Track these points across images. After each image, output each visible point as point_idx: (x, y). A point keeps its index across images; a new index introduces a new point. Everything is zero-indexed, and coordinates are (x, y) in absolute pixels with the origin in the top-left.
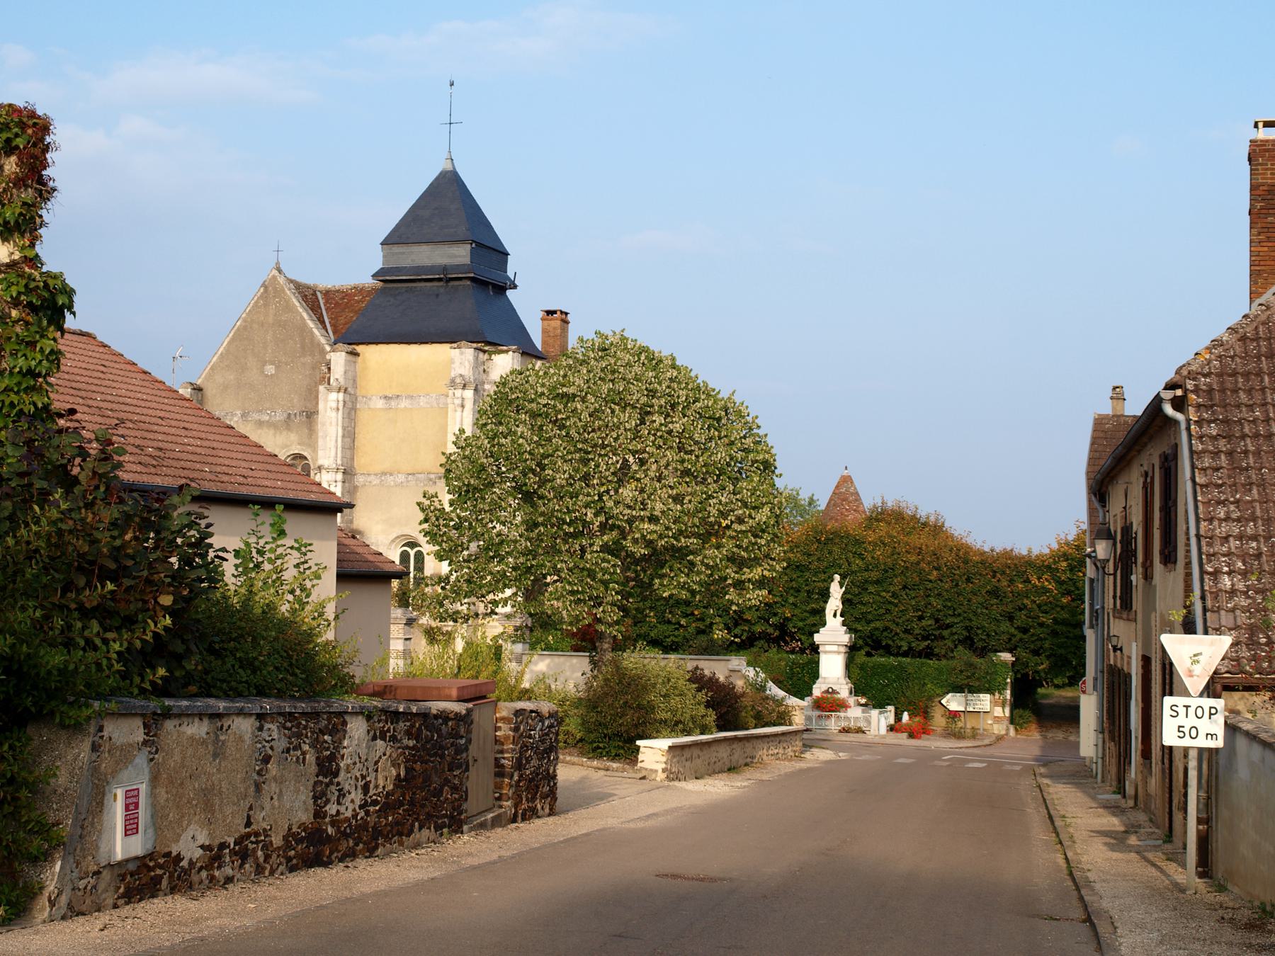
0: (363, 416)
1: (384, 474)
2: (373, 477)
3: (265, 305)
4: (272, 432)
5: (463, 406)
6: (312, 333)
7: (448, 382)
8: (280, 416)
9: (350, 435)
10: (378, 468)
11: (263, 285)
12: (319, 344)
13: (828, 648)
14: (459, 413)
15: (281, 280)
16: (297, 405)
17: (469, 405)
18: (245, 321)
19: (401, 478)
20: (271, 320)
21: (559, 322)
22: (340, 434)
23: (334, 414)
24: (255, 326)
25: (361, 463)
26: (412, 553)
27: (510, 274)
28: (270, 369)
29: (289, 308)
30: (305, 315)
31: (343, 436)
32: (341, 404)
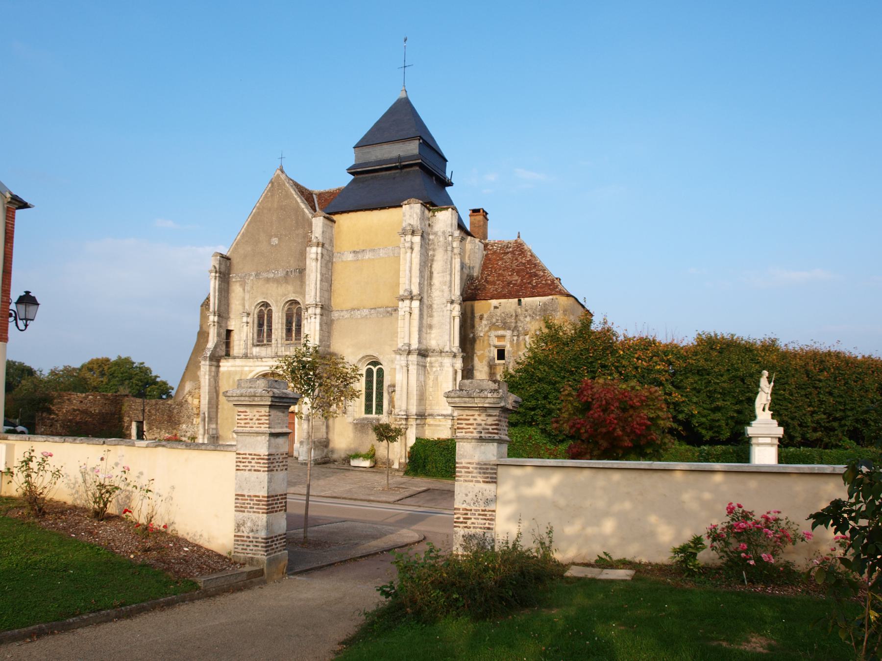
0: (338, 267)
2: (345, 313)
3: (272, 196)
4: (275, 285)
5: (412, 249)
6: (303, 212)
7: (400, 231)
8: (281, 273)
9: (327, 281)
10: (349, 305)
11: (271, 182)
13: (761, 440)
14: (409, 254)
15: (283, 177)
16: (293, 264)
17: (417, 248)
18: (258, 208)
21: (482, 217)
22: (319, 278)
23: (314, 264)
24: (265, 211)
25: (338, 301)
26: (375, 370)
27: (448, 175)
28: (275, 241)
29: (288, 196)
30: (299, 200)
31: (321, 280)
32: (319, 258)
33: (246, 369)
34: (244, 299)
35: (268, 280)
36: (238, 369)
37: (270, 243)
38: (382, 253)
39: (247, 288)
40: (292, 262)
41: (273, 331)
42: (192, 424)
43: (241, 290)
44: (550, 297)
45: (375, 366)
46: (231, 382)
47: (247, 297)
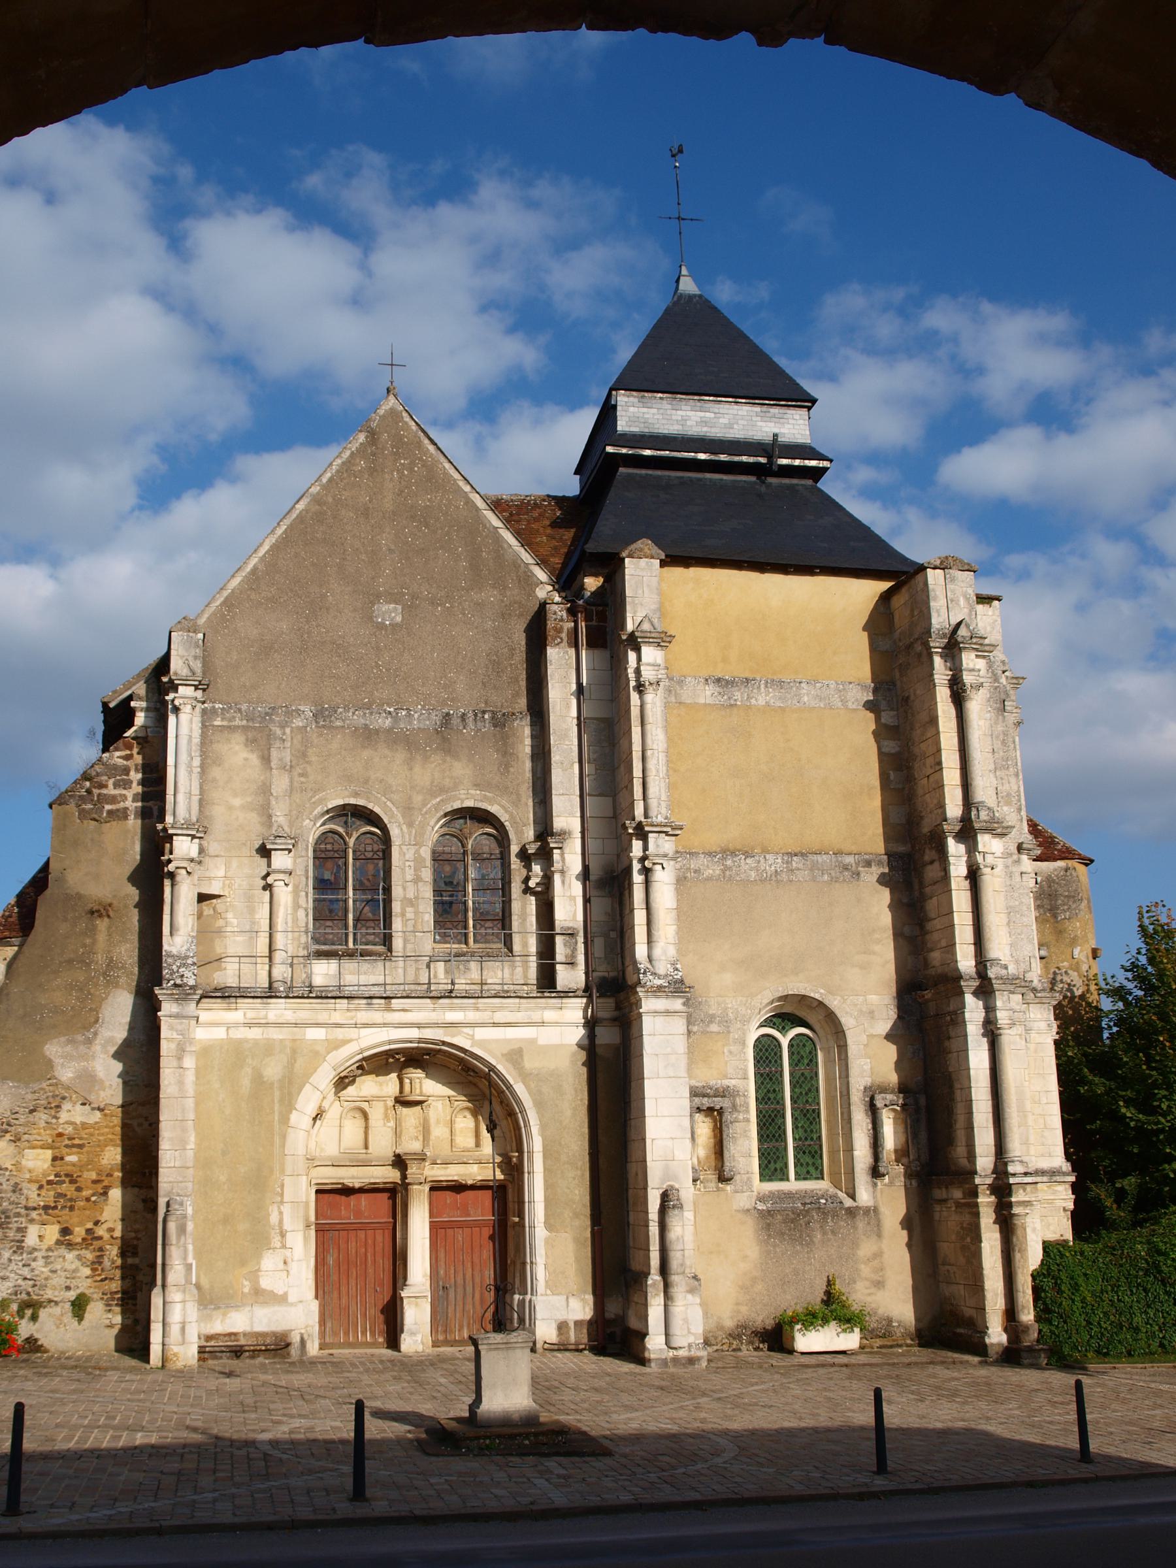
1: (728, 852)
4: (400, 756)
6: (498, 539)
8: (421, 719)
12: (517, 563)
19: (774, 863)
20: (388, 504)
28: (390, 613)
33: (315, 1034)
34: (265, 790)
35: (368, 736)
36: (276, 1034)
37: (371, 618)
38: (807, 695)
39: (281, 754)
40: (460, 687)
41: (396, 907)
42: (19, 1247)
43: (254, 759)
44: (1061, 864)
45: (783, 1030)
46: (246, 1083)
47: (280, 783)
